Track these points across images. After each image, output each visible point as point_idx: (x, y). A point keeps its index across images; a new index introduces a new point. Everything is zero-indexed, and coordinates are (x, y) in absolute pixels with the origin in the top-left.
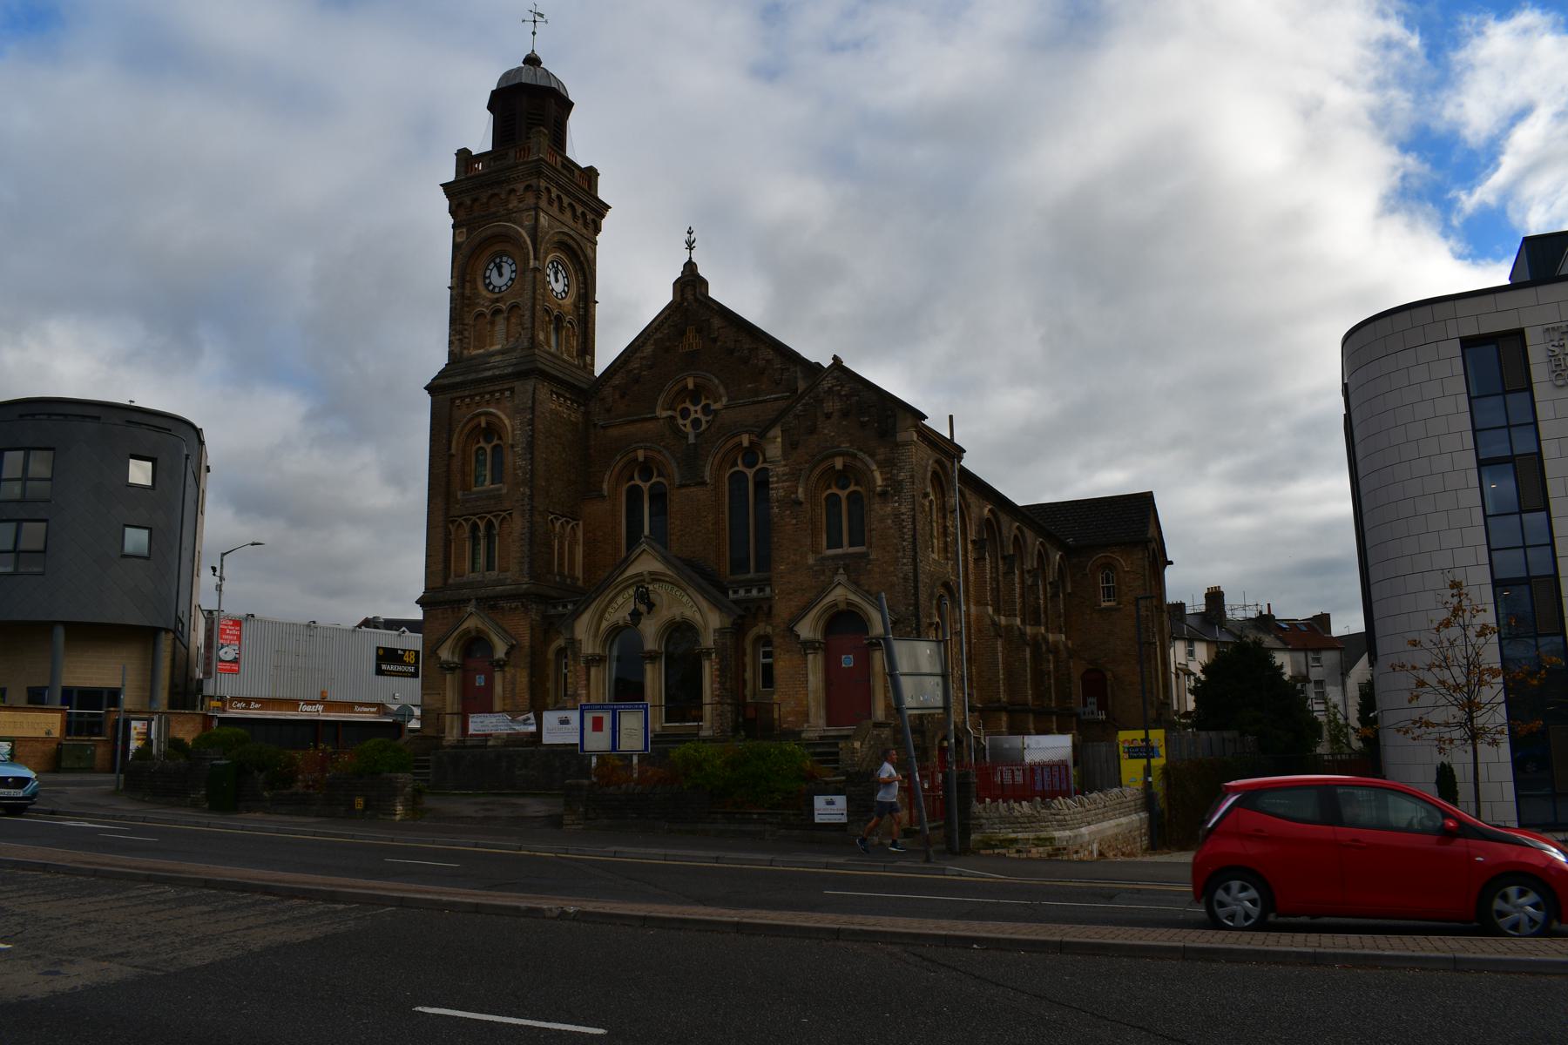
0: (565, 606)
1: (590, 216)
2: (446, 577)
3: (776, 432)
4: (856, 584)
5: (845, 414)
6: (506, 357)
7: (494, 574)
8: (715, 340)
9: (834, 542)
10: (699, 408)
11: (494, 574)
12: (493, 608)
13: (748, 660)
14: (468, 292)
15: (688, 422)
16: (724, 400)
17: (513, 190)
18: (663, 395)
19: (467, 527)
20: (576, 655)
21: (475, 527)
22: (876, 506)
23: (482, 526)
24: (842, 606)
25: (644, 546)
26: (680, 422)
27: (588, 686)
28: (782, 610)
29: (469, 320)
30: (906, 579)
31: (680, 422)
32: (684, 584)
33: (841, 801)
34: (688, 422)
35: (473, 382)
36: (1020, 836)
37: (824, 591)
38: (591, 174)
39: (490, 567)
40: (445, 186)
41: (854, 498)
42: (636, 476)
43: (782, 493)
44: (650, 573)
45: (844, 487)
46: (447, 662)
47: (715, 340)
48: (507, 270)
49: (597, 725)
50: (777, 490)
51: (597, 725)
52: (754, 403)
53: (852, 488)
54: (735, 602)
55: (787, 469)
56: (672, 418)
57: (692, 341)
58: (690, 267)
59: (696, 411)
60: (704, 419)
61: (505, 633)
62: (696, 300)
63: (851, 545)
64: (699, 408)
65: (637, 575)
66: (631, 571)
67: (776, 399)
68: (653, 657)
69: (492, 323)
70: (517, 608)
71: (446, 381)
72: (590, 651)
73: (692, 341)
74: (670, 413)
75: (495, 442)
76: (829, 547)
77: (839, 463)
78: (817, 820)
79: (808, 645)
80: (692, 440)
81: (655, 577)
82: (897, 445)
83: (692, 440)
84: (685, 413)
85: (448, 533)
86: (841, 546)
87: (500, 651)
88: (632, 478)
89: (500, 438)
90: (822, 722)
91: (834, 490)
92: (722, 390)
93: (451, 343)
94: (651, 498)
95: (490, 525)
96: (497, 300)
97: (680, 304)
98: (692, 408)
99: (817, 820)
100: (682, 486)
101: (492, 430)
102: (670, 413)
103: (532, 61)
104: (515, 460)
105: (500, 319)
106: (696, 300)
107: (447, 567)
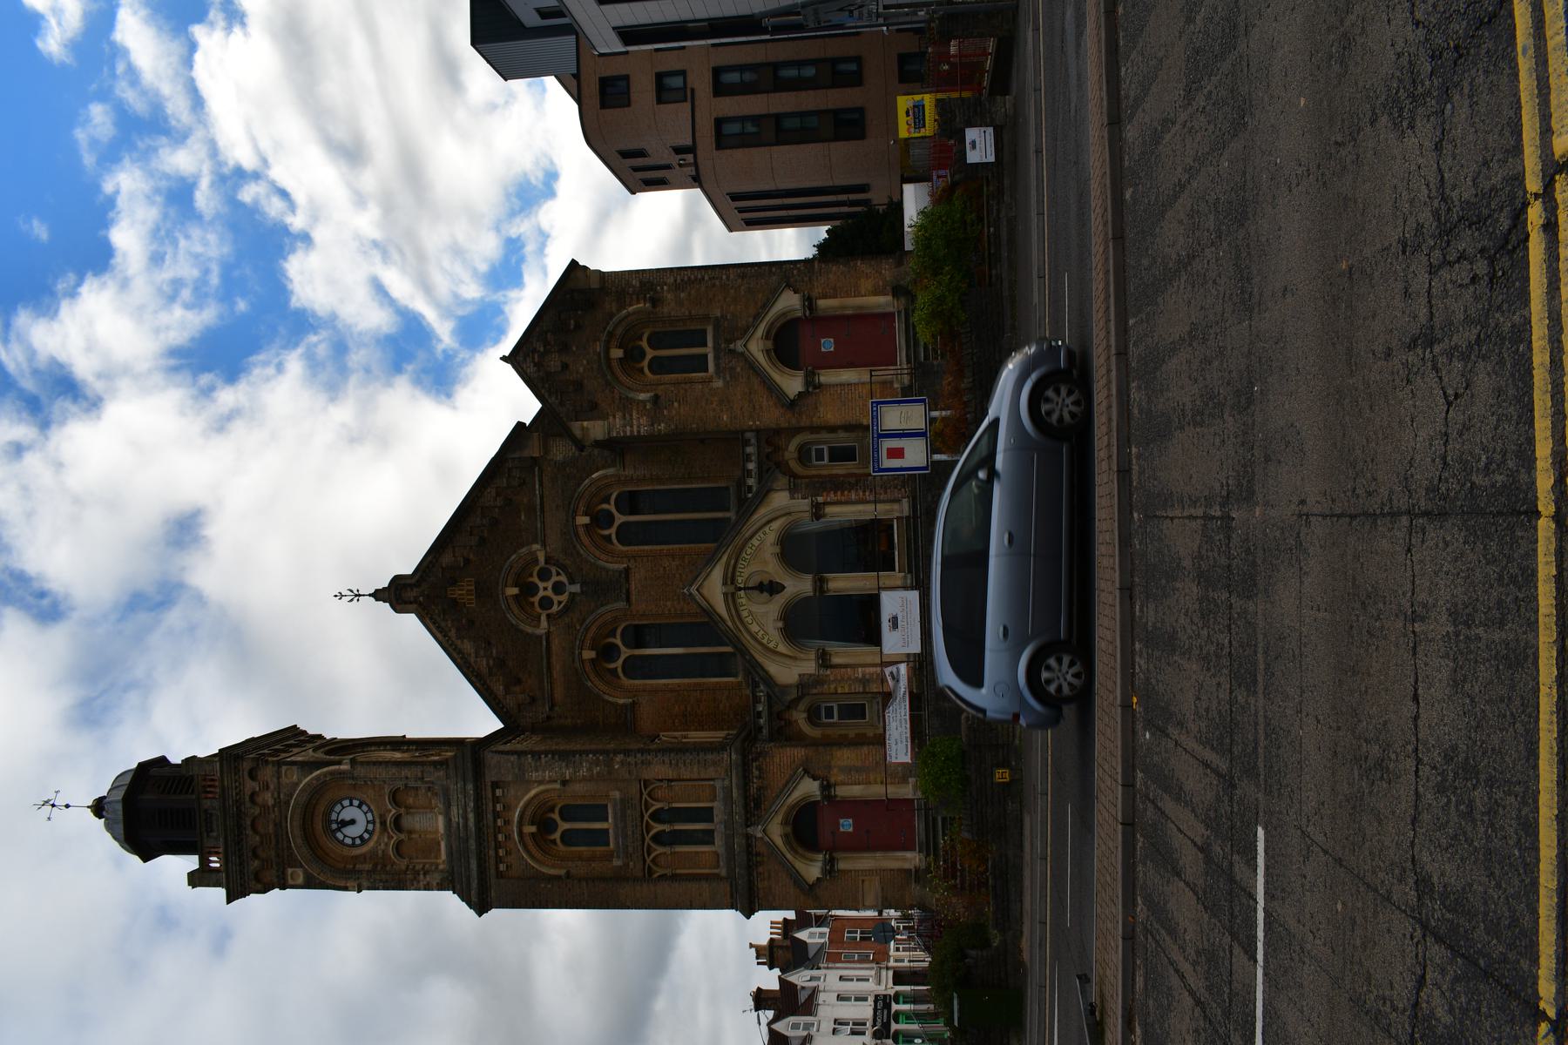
0: (759, 715)
2: (717, 877)
4: (746, 332)
5: (564, 348)
6: (454, 803)
7: (718, 806)
8: (467, 561)
9: (700, 363)
10: (541, 585)
11: (718, 806)
12: (758, 806)
13: (825, 472)
14: (368, 867)
15: (556, 599)
16: (536, 547)
18: (522, 626)
20: (817, 681)
21: (658, 839)
22: (666, 310)
24: (770, 344)
25: (693, 590)
27: (853, 666)
28: (772, 416)
29: (402, 864)
31: (555, 608)
32: (738, 541)
33: (971, 134)
35: (479, 843)
37: (752, 366)
39: (706, 815)
40: (230, 899)
42: (612, 666)
43: (644, 421)
44: (725, 584)
45: (643, 354)
46: (824, 871)
47: (467, 561)
48: (347, 814)
50: (640, 425)
53: (644, 344)
55: (619, 415)
56: (548, 616)
58: (378, 595)
59: (545, 589)
61: (791, 783)
62: (418, 584)
63: (705, 345)
64: (541, 585)
65: (726, 601)
66: (721, 609)
67: (541, 484)
69: (410, 832)
70: (759, 768)
72: (813, 664)
73: (463, 592)
75: (556, 816)
76: (706, 370)
77: (617, 353)
78: (991, 159)
79: (812, 385)
80: (576, 588)
81: (730, 578)
83: (576, 588)
84: (546, 603)
87: (809, 788)
89: (552, 810)
90: (891, 370)
91: (645, 363)
92: (524, 550)
93: (427, 888)
94: (639, 645)
95: (656, 817)
96: (383, 823)
97: (420, 604)
98: (541, 593)
99: (991, 159)
100: (628, 600)
102: (543, 618)
103: (99, 808)
105: (407, 822)
106: (418, 584)
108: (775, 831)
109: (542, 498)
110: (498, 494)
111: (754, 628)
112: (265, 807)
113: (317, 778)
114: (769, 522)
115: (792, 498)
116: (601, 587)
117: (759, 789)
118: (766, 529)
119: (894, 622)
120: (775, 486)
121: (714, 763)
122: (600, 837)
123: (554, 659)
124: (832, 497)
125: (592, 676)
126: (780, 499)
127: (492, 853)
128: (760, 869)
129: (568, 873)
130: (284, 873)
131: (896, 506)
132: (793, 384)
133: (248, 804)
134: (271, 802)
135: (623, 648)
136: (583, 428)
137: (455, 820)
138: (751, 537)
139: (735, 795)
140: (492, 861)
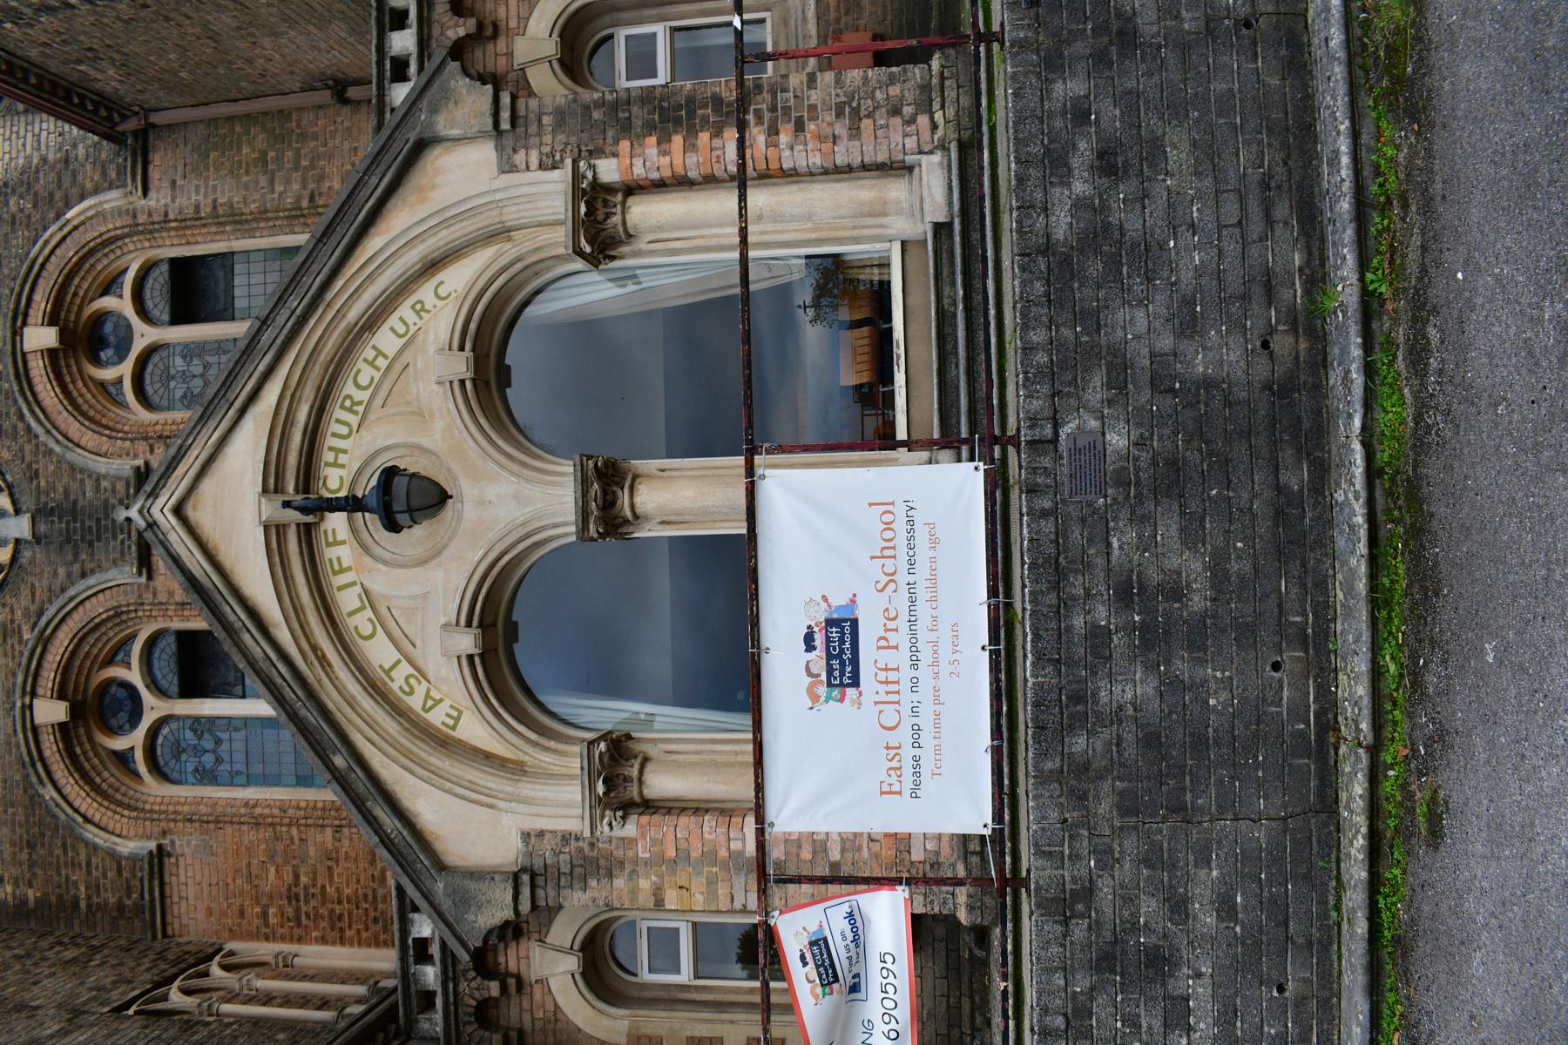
25: (162, 510)
44: (272, 484)
66: (257, 582)
88: (123, 759)
94: (190, 689)
111: (379, 653)
114: (432, 266)
115: (508, 167)
118: (425, 293)
119: (839, 649)
120: (443, 125)
124: (649, 159)
125: (60, 771)
126: (464, 174)
131: (896, 190)
135: (147, 697)
138: (372, 322)
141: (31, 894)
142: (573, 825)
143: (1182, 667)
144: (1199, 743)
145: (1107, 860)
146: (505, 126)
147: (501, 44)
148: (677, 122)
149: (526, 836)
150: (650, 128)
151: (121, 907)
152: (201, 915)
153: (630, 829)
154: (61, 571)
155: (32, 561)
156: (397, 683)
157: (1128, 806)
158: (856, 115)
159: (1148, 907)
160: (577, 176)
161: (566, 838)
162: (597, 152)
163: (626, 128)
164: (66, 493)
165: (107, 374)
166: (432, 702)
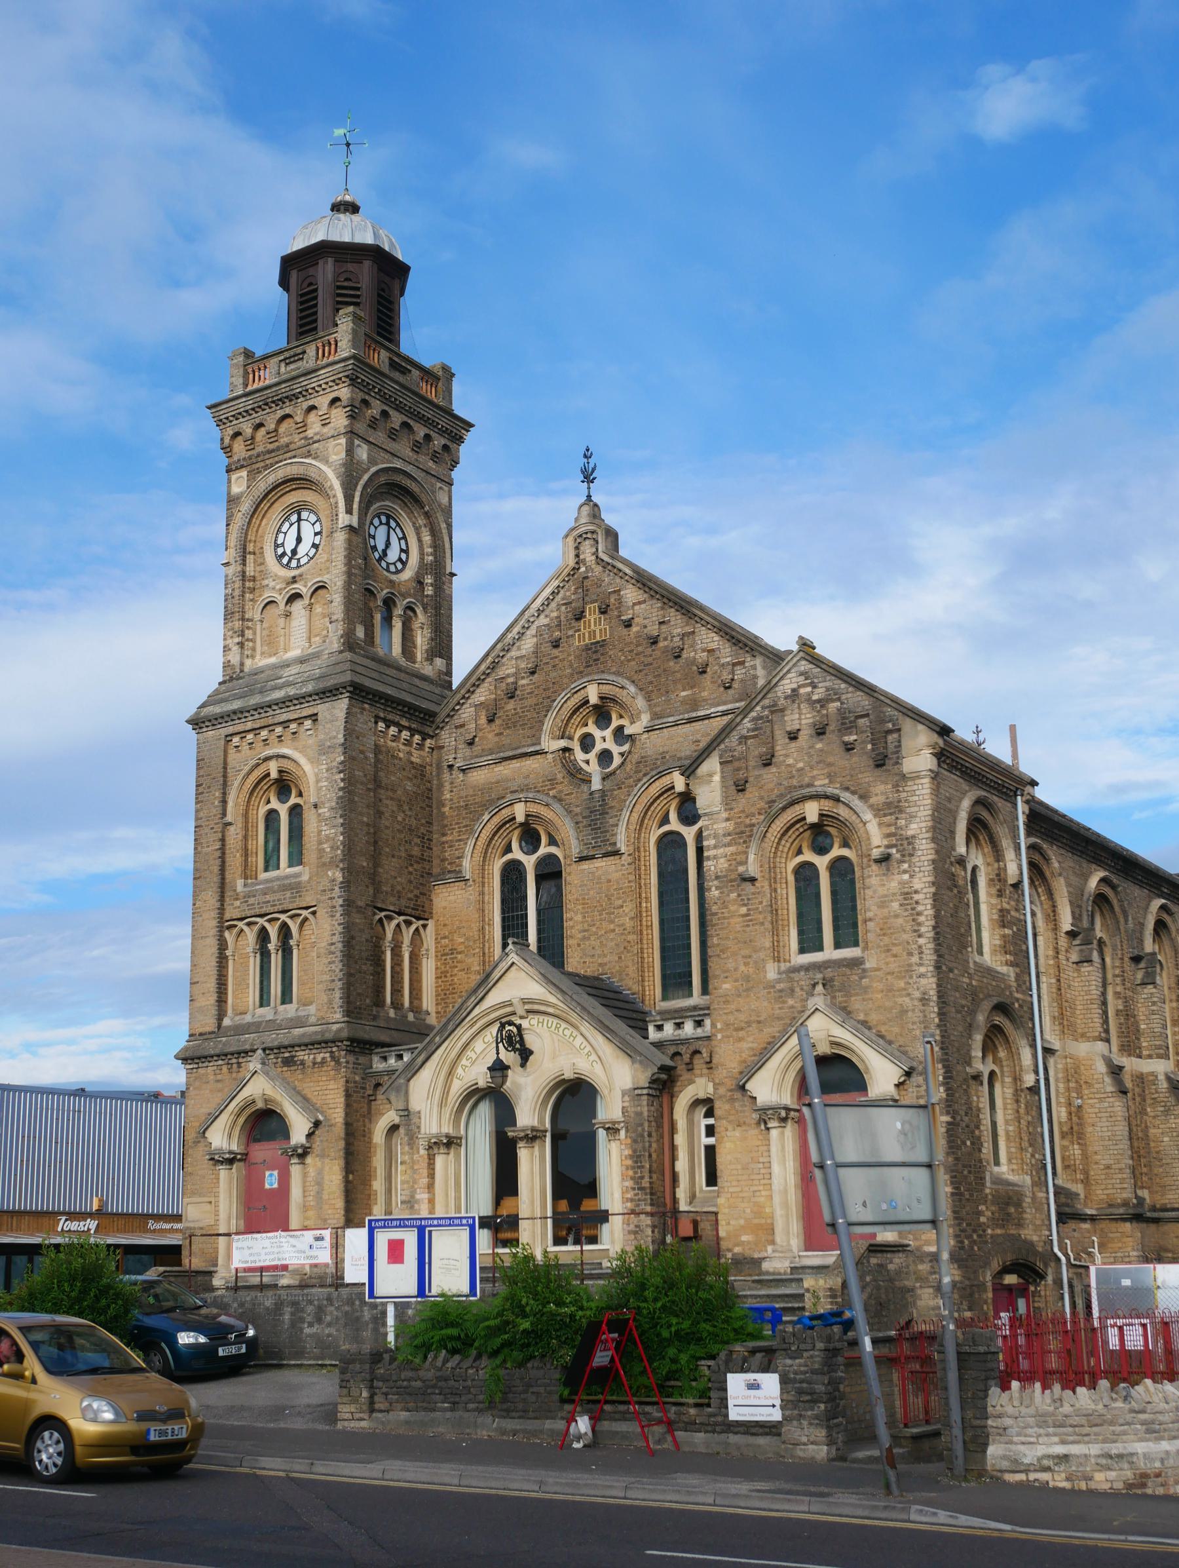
1: (438, 442)
2: (221, 1015)
3: (712, 765)
4: (845, 1013)
5: (820, 732)
6: (305, 667)
7: (290, 1010)
8: (628, 624)
10: (608, 733)
11: (290, 1010)
12: (288, 1062)
13: (680, 1139)
14: (250, 570)
15: (592, 756)
17: (313, 408)
18: (552, 715)
19: (251, 935)
20: (412, 1138)
21: (263, 936)
22: (874, 881)
23: (273, 931)
26: (580, 756)
27: (430, 1187)
28: (730, 1055)
29: (254, 612)
30: (924, 1000)
31: (580, 756)
32: (574, 1017)
33: (770, 1383)
34: (592, 756)
35: (258, 708)
36: (1074, 1449)
38: (442, 377)
39: (286, 997)
41: (842, 870)
42: (515, 845)
44: (524, 1001)
45: (822, 850)
46: (220, 1151)
49: (396, 1251)
51: (396, 1251)
52: (691, 721)
53: (836, 852)
54: (659, 1045)
55: (730, 826)
56: (566, 750)
57: (595, 626)
59: (604, 738)
60: (616, 750)
61: (305, 1102)
63: (838, 945)
64: (608, 733)
66: (493, 998)
68: (533, 1137)
69: (288, 615)
71: (217, 709)
72: (434, 1130)
73: (595, 626)
74: (563, 743)
76: (802, 951)
78: (734, 1415)
79: (766, 1116)
80: (596, 785)
81: (533, 1009)
82: (904, 777)
83: (596, 785)
84: (587, 743)
85: (222, 946)
86: (820, 948)
88: (508, 849)
90: (796, 1242)
92: (640, 703)
95: (285, 932)
96: (294, 580)
99: (734, 1415)
100: (582, 859)
101: (283, 786)
102: (563, 743)
104: (324, 830)
105: (298, 607)
107: (221, 1000)
108: (260, 1086)
109: (707, 717)
110: (711, 651)
112: (304, 426)
113: (332, 488)
116: (596, 818)
117: (303, 1063)
118: (593, 1057)
121: (330, 1002)
122: (271, 861)
123: (515, 764)
125: (496, 820)
127: (249, 726)
128: (225, 1068)
129: (230, 824)
130: (242, 467)
132: (771, 1086)
133: (305, 405)
134: (310, 433)
136: (711, 775)
137: (286, 672)
139: (297, 1032)
140: (240, 728)
141: (446, 809)
142: (423, 1131)
143: (371, 1326)
144: (357, 1330)
145: (337, 1309)
146: (637, 1092)
147: (705, 1071)
148: (636, 1162)
149: (419, 1112)
150: (635, 1151)
151: (443, 860)
152: (444, 904)
153: (423, 1152)
154: (578, 810)
155: (583, 792)
156: (469, 1053)
157: (347, 1313)
158: (635, 1233)
159: (328, 1318)
160: (619, 1123)
161: (419, 1127)
162: (627, 1131)
163: (635, 1141)
164: (611, 808)
165: (673, 816)
166: (464, 1068)
